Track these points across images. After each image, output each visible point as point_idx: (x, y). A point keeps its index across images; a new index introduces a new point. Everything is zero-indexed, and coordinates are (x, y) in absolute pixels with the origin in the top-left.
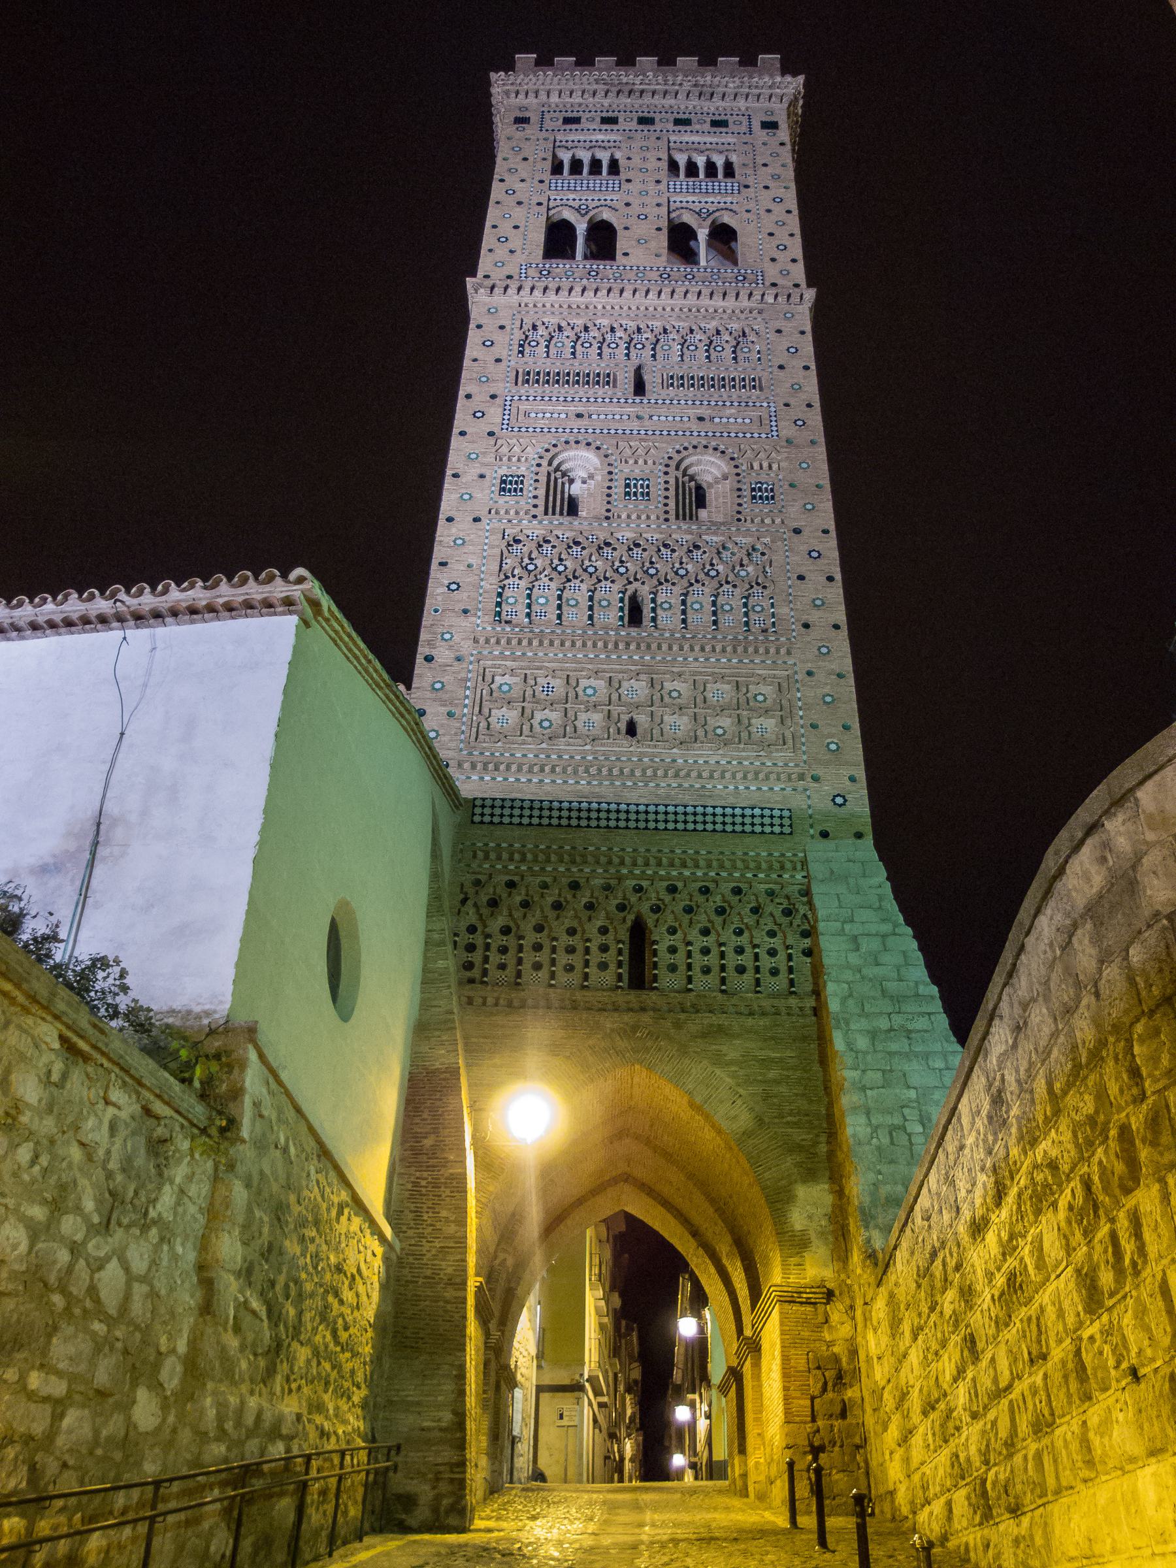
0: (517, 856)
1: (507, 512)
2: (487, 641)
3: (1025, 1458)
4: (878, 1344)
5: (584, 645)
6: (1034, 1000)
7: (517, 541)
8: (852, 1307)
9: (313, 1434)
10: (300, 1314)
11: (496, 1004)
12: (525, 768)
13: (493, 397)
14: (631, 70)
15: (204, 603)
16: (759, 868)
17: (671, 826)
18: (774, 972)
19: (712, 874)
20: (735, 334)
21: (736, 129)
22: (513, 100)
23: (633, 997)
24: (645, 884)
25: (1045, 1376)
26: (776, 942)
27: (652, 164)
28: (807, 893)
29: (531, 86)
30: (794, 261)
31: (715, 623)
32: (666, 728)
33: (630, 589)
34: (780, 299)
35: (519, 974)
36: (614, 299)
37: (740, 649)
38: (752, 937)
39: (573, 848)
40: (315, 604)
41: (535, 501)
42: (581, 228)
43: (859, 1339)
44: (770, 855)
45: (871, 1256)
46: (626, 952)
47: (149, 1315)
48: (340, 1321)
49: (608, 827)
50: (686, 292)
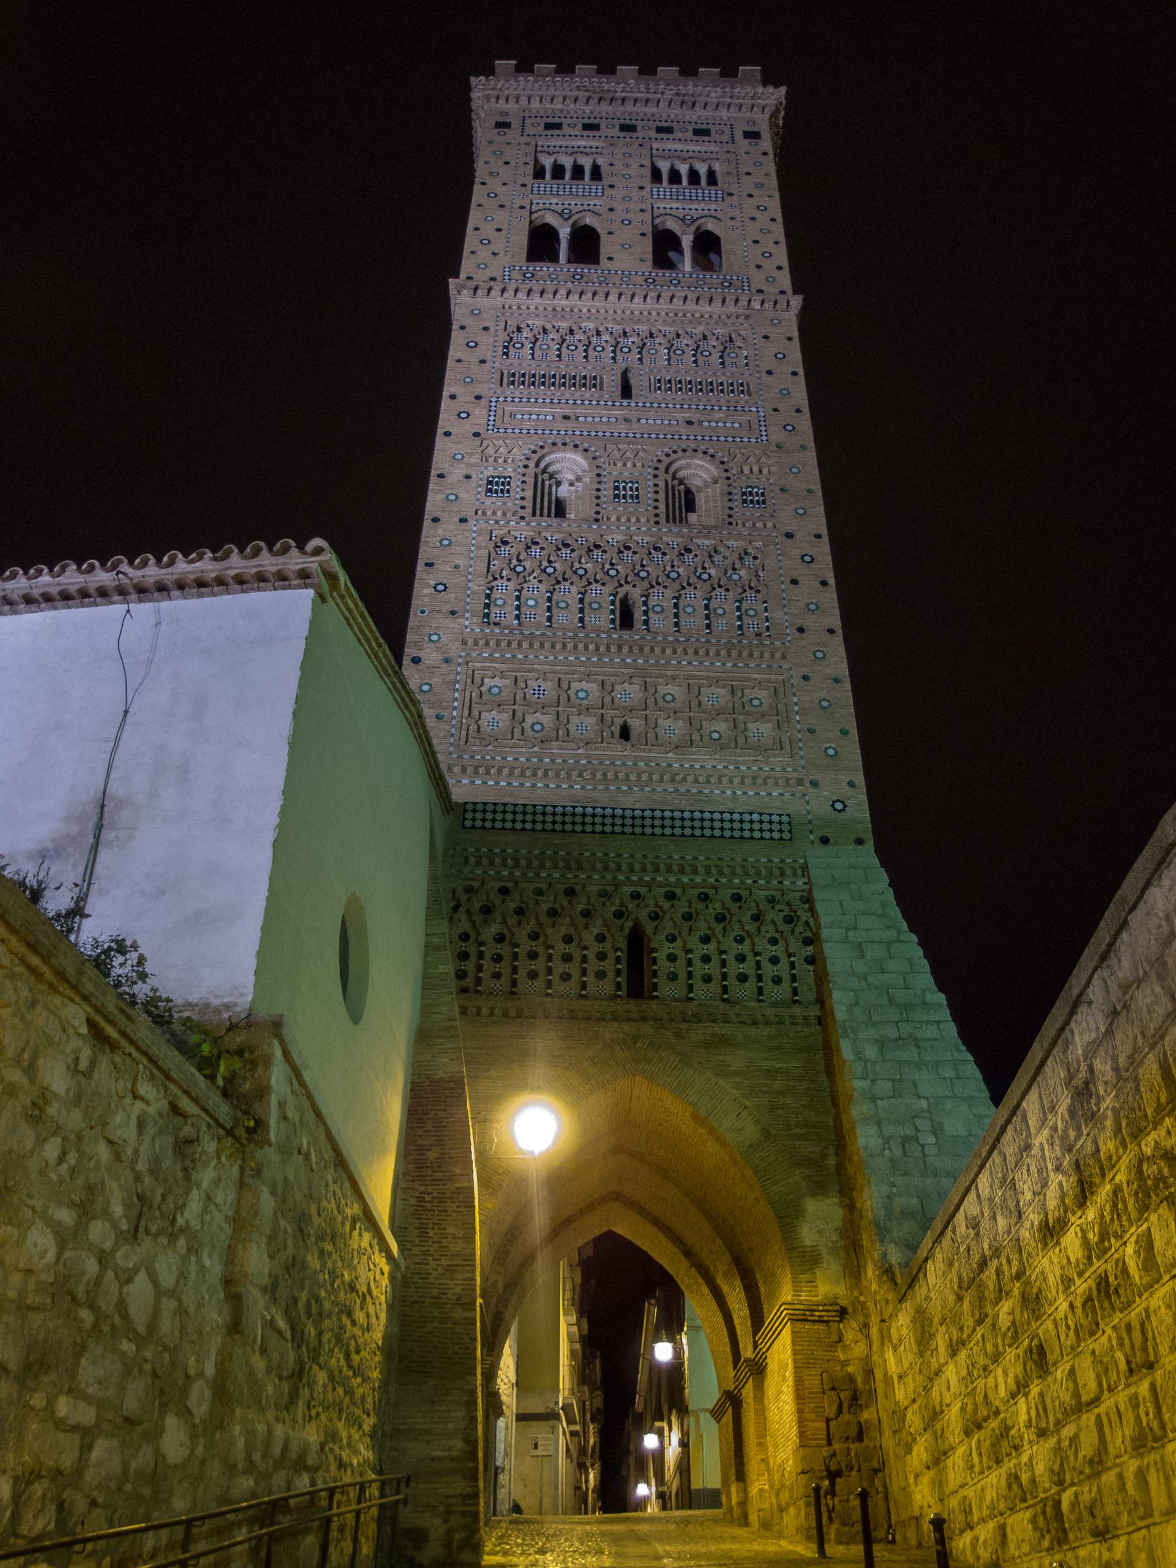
0: (510, 862)
1: (494, 513)
2: (476, 643)
3: (1121, 1477)
4: (900, 1361)
5: (576, 647)
6: (1139, 982)
7: (505, 543)
8: (866, 1325)
9: (333, 1467)
10: (320, 1335)
11: (491, 1014)
12: (517, 771)
13: (478, 398)
14: (613, 78)
15: (213, 575)
16: (759, 874)
17: (668, 831)
18: (777, 981)
19: (712, 880)
20: (722, 339)
21: (718, 138)
23: (632, 1006)
25: (1153, 1386)
26: (778, 950)
27: (635, 170)
28: (808, 899)
29: (511, 92)
30: (779, 268)
31: (708, 626)
32: (661, 732)
33: (622, 592)
34: (766, 305)
35: (514, 983)
36: (599, 302)
37: (734, 653)
38: (753, 944)
39: (568, 854)
40: (331, 577)
41: (523, 503)
42: (564, 232)
43: (875, 1358)
44: (770, 861)
45: (887, 1271)
46: (624, 961)
47: (177, 1334)
48: (353, 1343)
49: (603, 832)
50: (672, 297)
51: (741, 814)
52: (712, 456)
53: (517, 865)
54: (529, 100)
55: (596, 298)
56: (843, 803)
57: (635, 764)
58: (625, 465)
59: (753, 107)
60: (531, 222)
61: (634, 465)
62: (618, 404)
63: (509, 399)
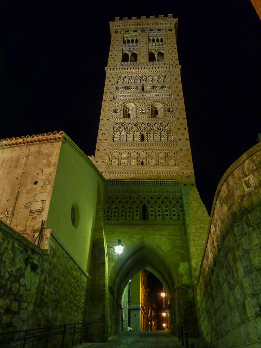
1: (115, 118)
2: (111, 146)
5: (132, 146)
7: (117, 124)
11: (114, 224)
13: (111, 93)
15: (41, 139)
16: (170, 192)
18: (174, 215)
19: (160, 194)
20: (164, 76)
21: (163, 31)
22: (115, 28)
23: (144, 222)
24: (146, 197)
26: (174, 209)
27: (145, 40)
28: (181, 198)
33: (142, 133)
35: (119, 217)
36: (137, 70)
40: (65, 138)
41: (121, 115)
42: (130, 55)
46: (142, 212)
51: (167, 180)
52: (161, 102)
53: (119, 192)
54: (122, 26)
55: (137, 69)
58: (142, 105)
59: (171, 23)
60: (123, 53)
61: (145, 105)
62: (141, 92)
63: (118, 93)
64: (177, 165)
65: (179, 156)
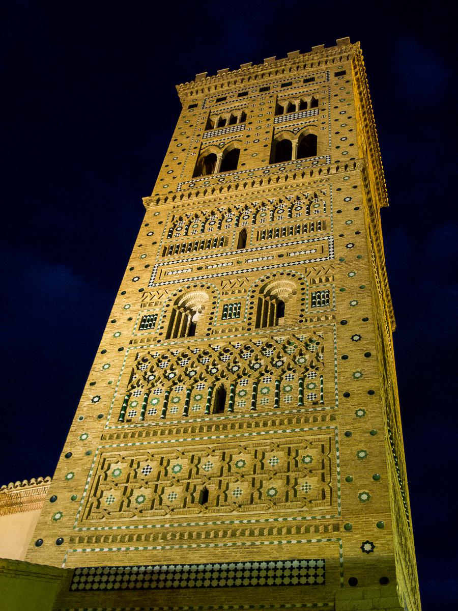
7: (145, 360)
22: (190, 98)
29: (199, 88)
33: (218, 384)
52: (294, 276)
55: (231, 190)
56: (372, 544)
57: (206, 524)
60: (199, 155)
64: (328, 496)
65: (338, 461)
